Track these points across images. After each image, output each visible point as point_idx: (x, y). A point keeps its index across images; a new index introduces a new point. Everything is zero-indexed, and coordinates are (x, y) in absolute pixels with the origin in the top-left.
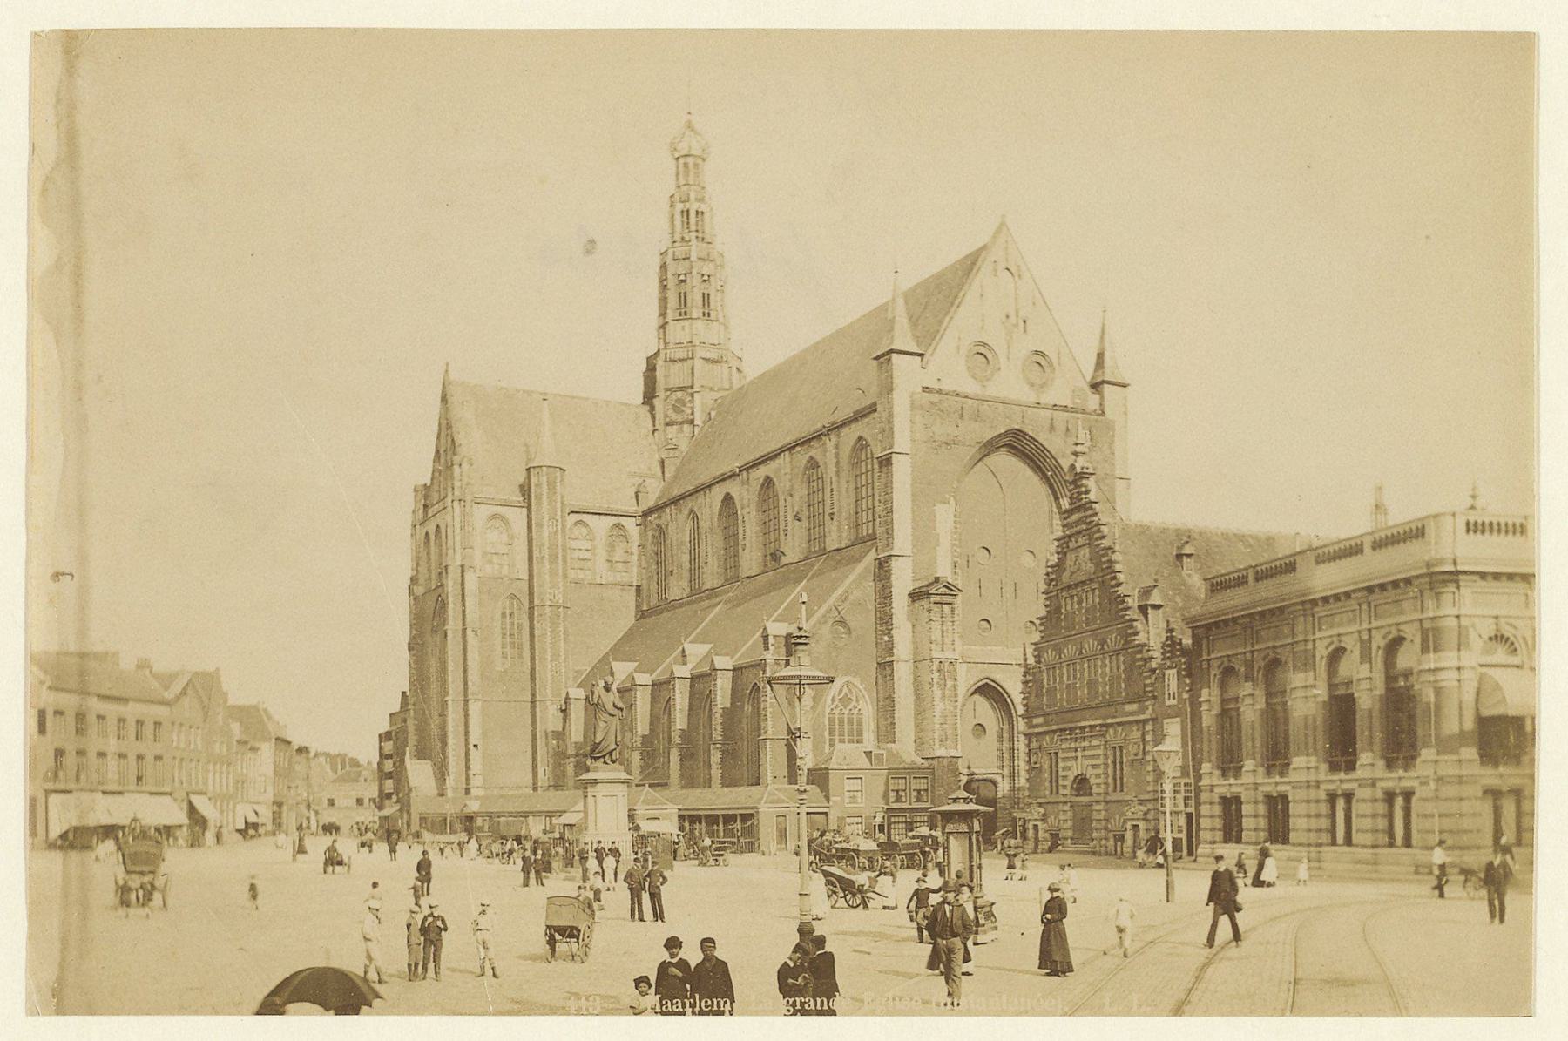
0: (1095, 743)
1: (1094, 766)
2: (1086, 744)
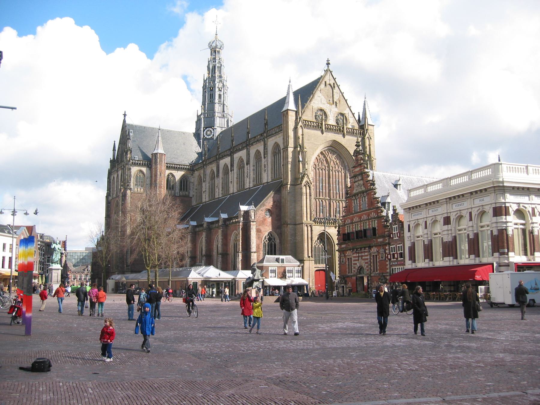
0: (366, 254)
1: (366, 263)
2: (363, 254)
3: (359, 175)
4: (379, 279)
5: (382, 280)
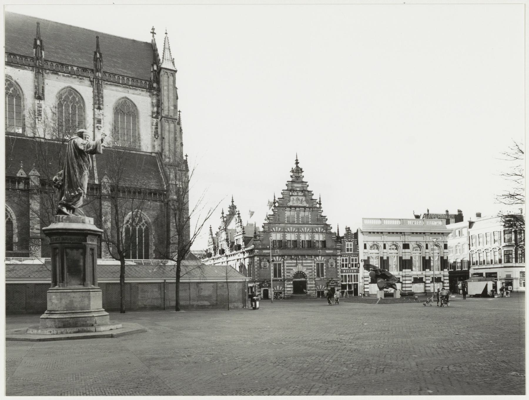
1: (307, 269)
3: (300, 191)
5: (333, 283)
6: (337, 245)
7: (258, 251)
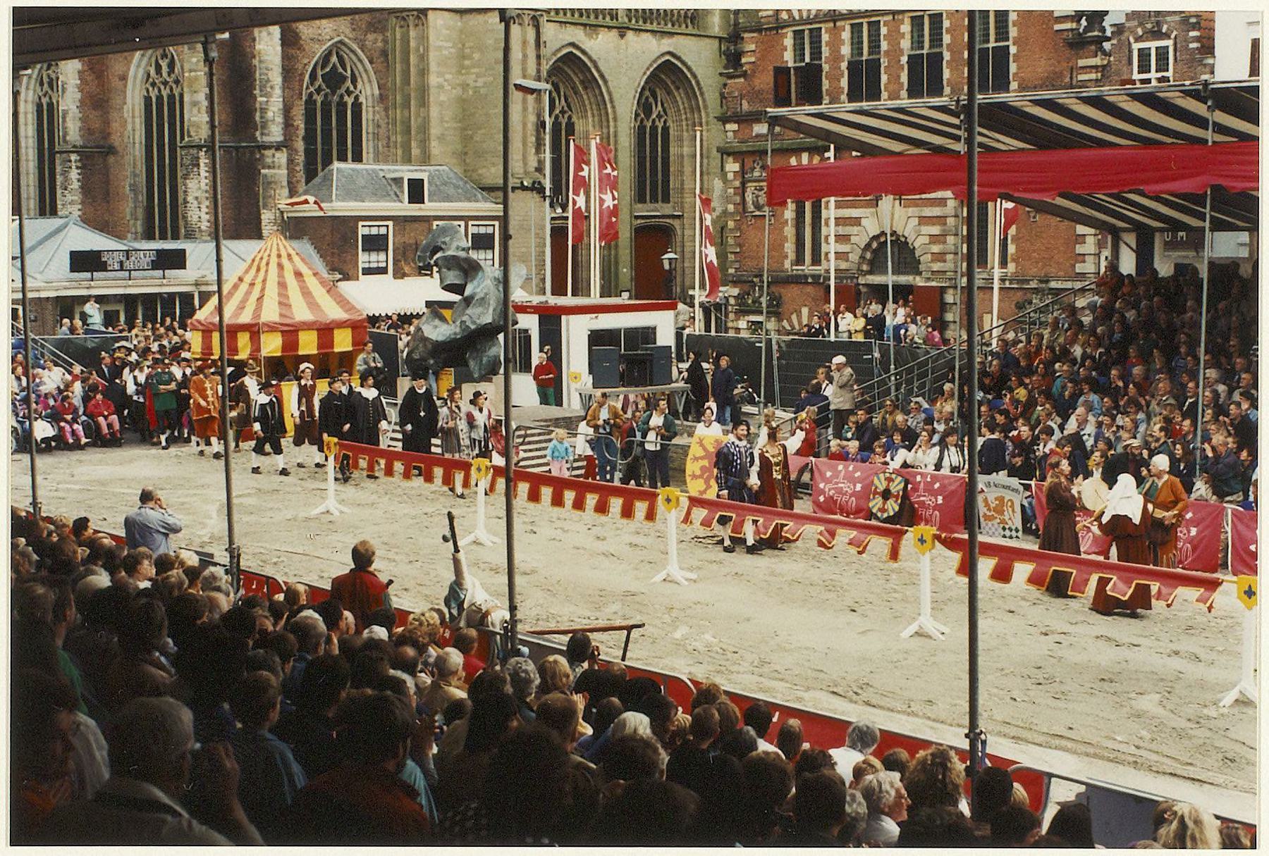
4: (1020, 306)
6: (1081, 63)
7: (735, 127)
